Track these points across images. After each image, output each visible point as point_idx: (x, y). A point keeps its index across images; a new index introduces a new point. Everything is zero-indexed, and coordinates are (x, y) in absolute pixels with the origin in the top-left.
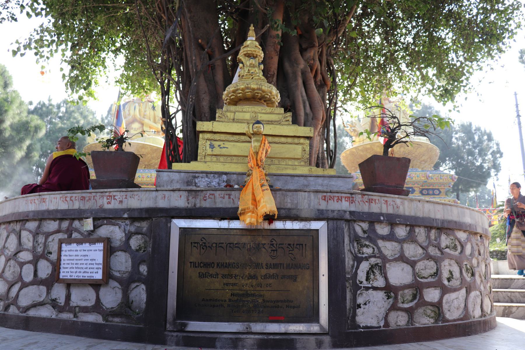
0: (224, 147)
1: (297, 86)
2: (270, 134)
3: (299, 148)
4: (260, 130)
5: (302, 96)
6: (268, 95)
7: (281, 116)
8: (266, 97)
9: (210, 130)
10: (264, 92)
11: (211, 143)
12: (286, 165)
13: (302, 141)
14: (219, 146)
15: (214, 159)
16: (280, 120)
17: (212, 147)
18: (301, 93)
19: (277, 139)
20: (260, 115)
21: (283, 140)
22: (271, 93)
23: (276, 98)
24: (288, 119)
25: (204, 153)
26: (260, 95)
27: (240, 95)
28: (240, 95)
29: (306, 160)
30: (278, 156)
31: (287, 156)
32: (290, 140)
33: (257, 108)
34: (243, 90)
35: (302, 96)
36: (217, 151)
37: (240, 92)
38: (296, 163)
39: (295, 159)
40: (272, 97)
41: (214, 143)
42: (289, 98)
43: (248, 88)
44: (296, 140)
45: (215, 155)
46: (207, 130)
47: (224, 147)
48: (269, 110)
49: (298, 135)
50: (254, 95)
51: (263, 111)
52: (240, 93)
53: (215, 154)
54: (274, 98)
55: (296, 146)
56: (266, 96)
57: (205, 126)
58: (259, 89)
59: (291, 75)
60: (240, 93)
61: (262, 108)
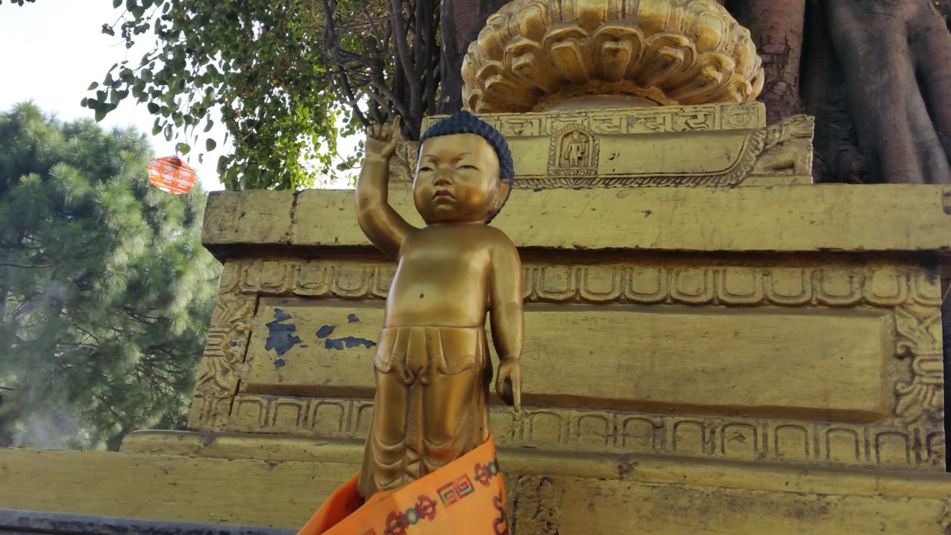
0: (352, 342)
1: (889, 88)
2: (646, 245)
3: (864, 341)
4: (458, 183)
5: (914, 130)
6: (676, 44)
7: (736, 145)
8: (669, 62)
9: (274, 238)
10: (649, 26)
11: (281, 316)
12: (760, 464)
13: (883, 283)
14: (325, 331)
15: (286, 412)
16: (734, 169)
17: (282, 337)
18: (911, 118)
19: (693, 282)
20: (606, 148)
21: (739, 281)
22: (695, 36)
23: (730, 63)
24: (785, 157)
25: (229, 381)
26: (626, 46)
27: (522, 60)
28: (522, 60)
29: (923, 429)
30: (702, 393)
31: (765, 398)
32: (787, 283)
33: (602, 117)
34: (535, 30)
35: (914, 130)
36: (308, 364)
37: (525, 41)
38: (843, 452)
39: (828, 416)
40: (703, 59)
41: (296, 312)
42: (856, 144)
43: (559, 19)
44: (838, 284)
45: (298, 392)
46: (256, 239)
47: (352, 342)
48: (669, 115)
49: (850, 243)
50: (595, 52)
51: (638, 129)
52: (520, 52)
53: (293, 380)
54: (718, 65)
55: (834, 321)
56: (668, 51)
57: (252, 215)
58: (612, 16)
59: (861, 49)
60: (520, 52)
61: (633, 111)
